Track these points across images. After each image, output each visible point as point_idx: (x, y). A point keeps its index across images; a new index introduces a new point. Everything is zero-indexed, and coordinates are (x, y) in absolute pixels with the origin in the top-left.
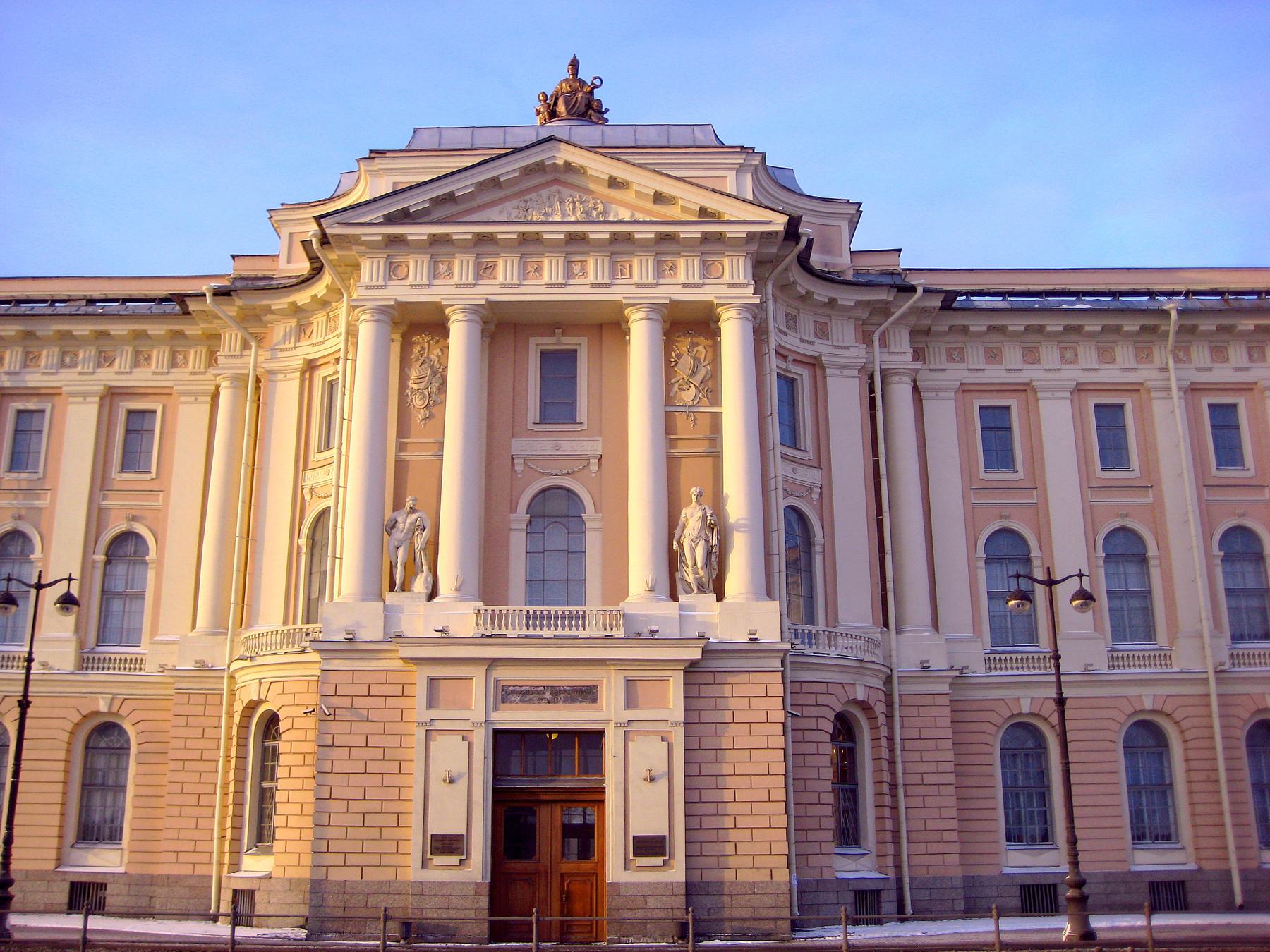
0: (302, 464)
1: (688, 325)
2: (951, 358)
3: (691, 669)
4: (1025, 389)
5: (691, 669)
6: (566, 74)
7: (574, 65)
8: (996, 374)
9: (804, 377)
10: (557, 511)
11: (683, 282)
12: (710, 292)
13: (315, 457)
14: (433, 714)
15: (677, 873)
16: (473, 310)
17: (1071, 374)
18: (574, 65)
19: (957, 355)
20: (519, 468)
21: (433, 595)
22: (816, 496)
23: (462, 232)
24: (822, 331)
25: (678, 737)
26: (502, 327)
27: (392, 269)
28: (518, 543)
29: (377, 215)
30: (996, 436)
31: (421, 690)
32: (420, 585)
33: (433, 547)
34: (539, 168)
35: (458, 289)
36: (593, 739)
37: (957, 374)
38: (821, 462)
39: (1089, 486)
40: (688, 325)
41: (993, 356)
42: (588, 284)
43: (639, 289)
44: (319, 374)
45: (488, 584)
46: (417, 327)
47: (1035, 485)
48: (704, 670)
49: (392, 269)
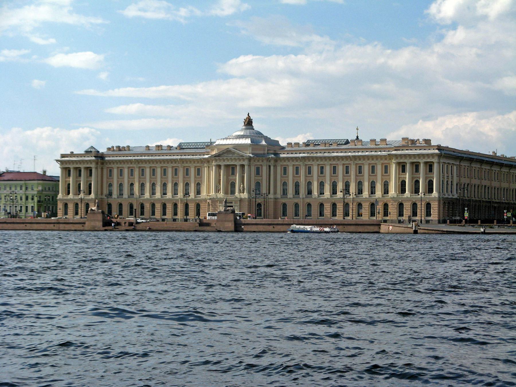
1: (243, 166)
6: (247, 116)
9: (260, 167)
10: (233, 185)
12: (243, 163)
23: (221, 158)
24: (263, 161)
26: (227, 166)
30: (285, 171)
37: (281, 163)
38: (262, 176)
40: (243, 166)
43: (238, 163)
45: (226, 193)
46: (219, 167)
47: (288, 177)
48: (241, 200)
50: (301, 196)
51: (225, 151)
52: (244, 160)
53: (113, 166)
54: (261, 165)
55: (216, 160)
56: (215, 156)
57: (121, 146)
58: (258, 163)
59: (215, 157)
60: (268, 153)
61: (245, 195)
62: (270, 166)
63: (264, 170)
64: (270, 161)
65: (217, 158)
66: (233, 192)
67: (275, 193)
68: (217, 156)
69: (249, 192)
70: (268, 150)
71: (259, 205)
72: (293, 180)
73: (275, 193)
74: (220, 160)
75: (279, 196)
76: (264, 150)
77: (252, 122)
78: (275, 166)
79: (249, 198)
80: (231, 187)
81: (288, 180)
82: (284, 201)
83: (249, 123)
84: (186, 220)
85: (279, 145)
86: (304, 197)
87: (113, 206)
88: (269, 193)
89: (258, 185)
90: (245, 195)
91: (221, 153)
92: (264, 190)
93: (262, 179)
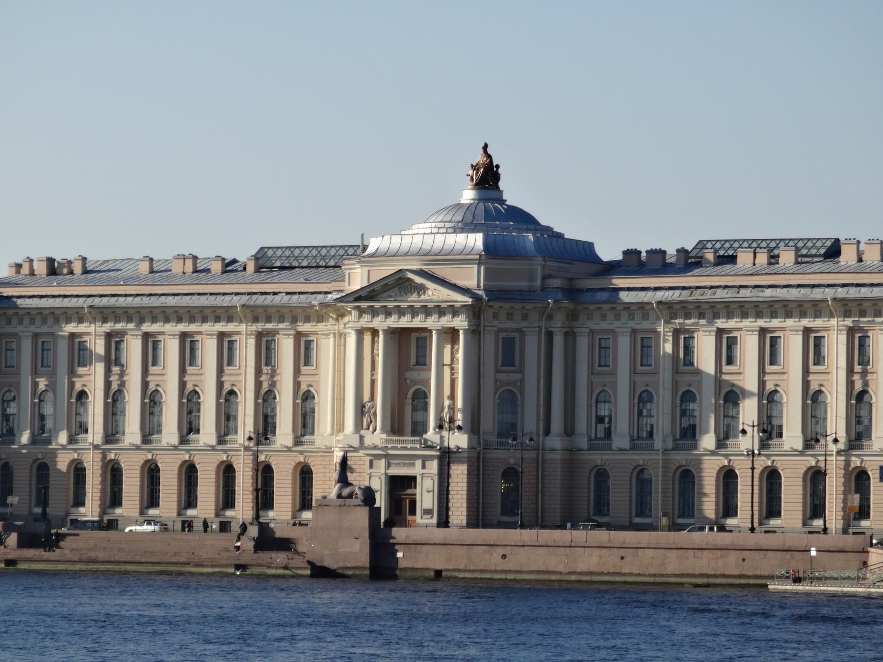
2: (588, 319)
4: (613, 331)
7: (485, 147)
8: (604, 325)
11: (446, 321)
14: (371, 471)
15: (435, 520)
16: (384, 330)
17: (632, 324)
18: (485, 147)
19: (590, 317)
20: (408, 381)
21: (375, 430)
22: (519, 383)
23: (377, 305)
24: (525, 317)
25: (436, 479)
27: (360, 316)
28: (408, 409)
29: (352, 298)
30: (603, 351)
31: (368, 463)
33: (375, 414)
34: (400, 278)
35: (381, 323)
36: (414, 478)
37: (591, 324)
38: (521, 371)
41: (604, 317)
42: (418, 322)
43: (433, 323)
47: (614, 373)
48: (446, 457)
49: (360, 316)
50: (658, 443)
51: (391, 281)
52: (454, 311)
53: (19, 329)
54: (519, 331)
55: (361, 312)
56: (358, 297)
57: (58, 257)
58: (510, 325)
59: (358, 299)
60: (543, 289)
61: (459, 440)
62: (550, 335)
63: (532, 347)
64: (550, 317)
65: (364, 305)
66: (419, 429)
67: (569, 431)
68: (369, 295)
69: (474, 427)
70: (544, 278)
71: (511, 474)
72: (633, 385)
73: (569, 431)
74: (374, 312)
75: (583, 443)
76: (532, 278)
77: (496, 177)
78: (570, 337)
79: (471, 448)
80: (414, 409)
81: (614, 385)
82: (598, 458)
83: (488, 177)
84: (224, 527)
85: (596, 260)
86: (670, 445)
87: (162, 474)
88: (547, 432)
89: (510, 400)
90: (459, 440)
91: (377, 287)
92: (530, 423)
93: (522, 381)
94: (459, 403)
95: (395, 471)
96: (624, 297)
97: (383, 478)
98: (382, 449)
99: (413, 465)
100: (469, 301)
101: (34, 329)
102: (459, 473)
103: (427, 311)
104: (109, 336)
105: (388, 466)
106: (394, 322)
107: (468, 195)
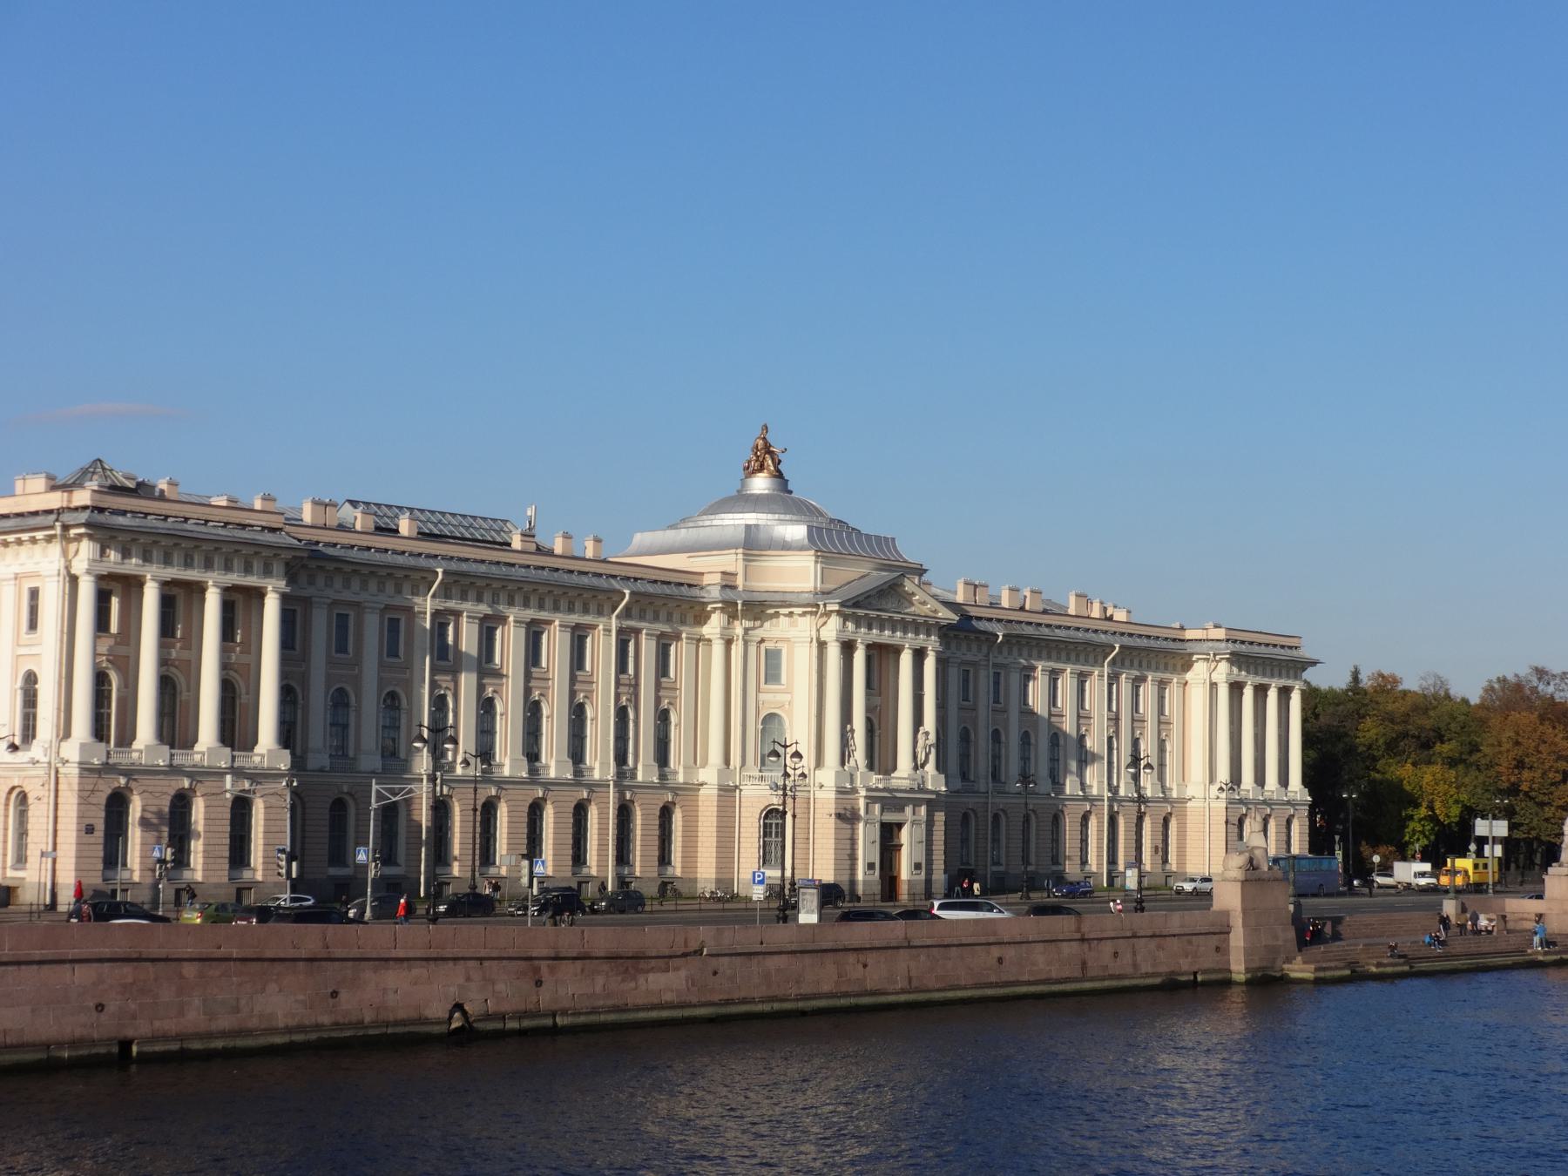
0: (758, 690)
3: (929, 802)
5: (929, 802)
13: (763, 686)
18: (766, 428)
32: (852, 762)
35: (863, 637)
39: (961, 708)
40: (919, 655)
43: (908, 643)
44: (763, 646)
46: (848, 648)
65: (861, 612)
74: (858, 622)
90: (934, 780)
94: (932, 738)
95: (891, 817)
96: (982, 626)
97: (878, 826)
98: (885, 790)
99: (903, 810)
100: (954, 618)
101: (384, 599)
102: (940, 817)
103: (905, 626)
104: (436, 614)
105: (882, 810)
106: (875, 635)
107: (761, 484)
